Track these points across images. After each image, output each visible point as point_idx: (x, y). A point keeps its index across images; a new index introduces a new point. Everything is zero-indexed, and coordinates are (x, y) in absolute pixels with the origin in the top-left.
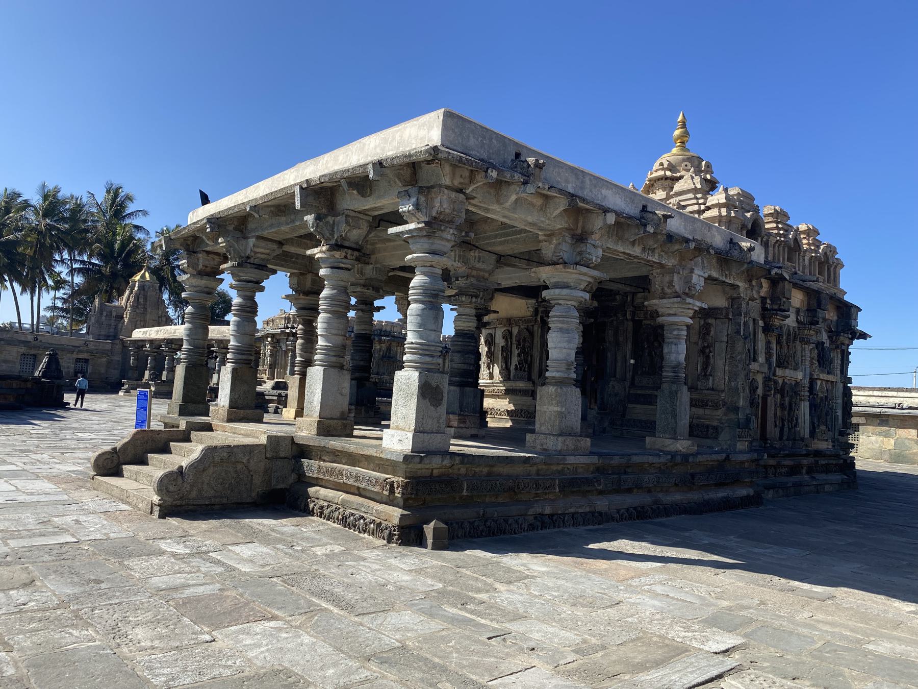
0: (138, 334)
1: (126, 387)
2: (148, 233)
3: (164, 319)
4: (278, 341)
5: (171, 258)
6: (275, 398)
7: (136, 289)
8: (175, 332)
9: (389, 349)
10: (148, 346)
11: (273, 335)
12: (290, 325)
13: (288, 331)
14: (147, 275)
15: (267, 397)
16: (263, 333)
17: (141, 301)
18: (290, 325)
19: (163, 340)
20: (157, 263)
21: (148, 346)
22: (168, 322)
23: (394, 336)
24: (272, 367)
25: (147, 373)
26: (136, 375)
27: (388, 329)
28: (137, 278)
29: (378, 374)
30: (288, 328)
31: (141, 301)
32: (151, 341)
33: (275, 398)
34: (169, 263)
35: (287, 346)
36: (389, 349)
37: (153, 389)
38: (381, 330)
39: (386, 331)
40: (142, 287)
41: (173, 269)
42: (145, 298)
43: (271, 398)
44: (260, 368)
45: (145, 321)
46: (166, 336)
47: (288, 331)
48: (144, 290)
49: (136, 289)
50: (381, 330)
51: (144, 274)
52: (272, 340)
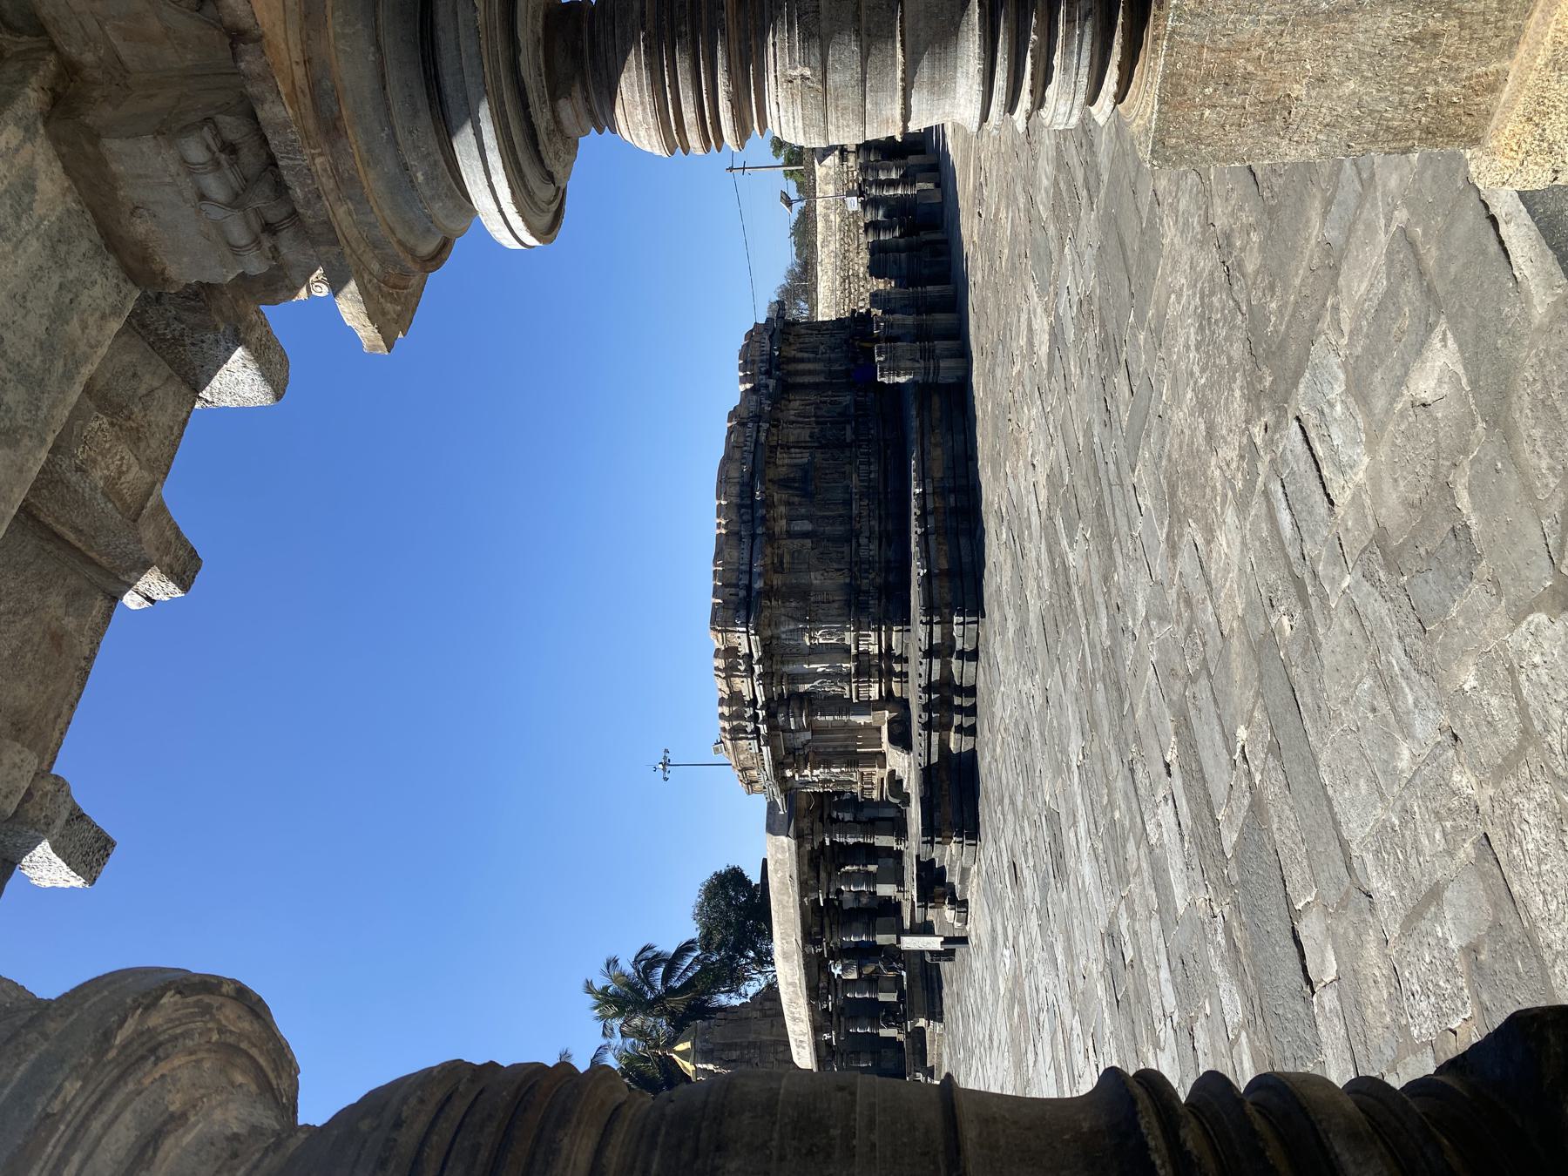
0: (804, 1056)
1: (920, 1077)
2: (602, 1050)
3: (768, 1005)
4: (791, 751)
5: (650, 996)
6: (935, 737)
7: (711, 1067)
8: (793, 984)
9: (784, 483)
10: (827, 1036)
11: (779, 766)
12: (750, 727)
13: (763, 729)
14: (680, 1047)
15: (935, 759)
16: (776, 790)
17: (735, 1055)
18: (750, 727)
19: (812, 1009)
20: (663, 1021)
21: (827, 1036)
22: (771, 994)
23: (752, 475)
24: (853, 760)
25: (885, 1032)
26: (889, 1053)
27: (735, 490)
28: (688, 1067)
29: (848, 503)
30: (757, 730)
31: (735, 1055)
32: (817, 1030)
33: (935, 737)
34: (659, 999)
35: (800, 729)
36: (784, 483)
37: (922, 1022)
38: (740, 506)
39: (741, 495)
40: (707, 1056)
41: (671, 992)
42: (730, 1046)
43: (935, 749)
44: (857, 789)
45: (775, 1043)
46: (803, 1001)
47: (763, 729)
48: (712, 1051)
49: (711, 1067)
50: (740, 506)
51: (679, 1053)
52: (790, 766)
